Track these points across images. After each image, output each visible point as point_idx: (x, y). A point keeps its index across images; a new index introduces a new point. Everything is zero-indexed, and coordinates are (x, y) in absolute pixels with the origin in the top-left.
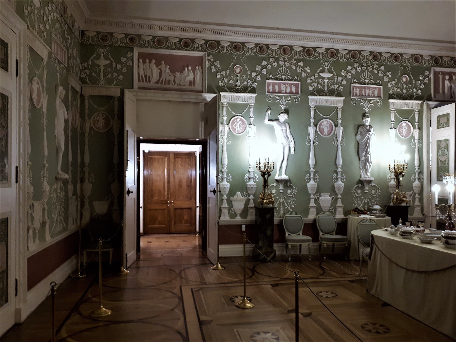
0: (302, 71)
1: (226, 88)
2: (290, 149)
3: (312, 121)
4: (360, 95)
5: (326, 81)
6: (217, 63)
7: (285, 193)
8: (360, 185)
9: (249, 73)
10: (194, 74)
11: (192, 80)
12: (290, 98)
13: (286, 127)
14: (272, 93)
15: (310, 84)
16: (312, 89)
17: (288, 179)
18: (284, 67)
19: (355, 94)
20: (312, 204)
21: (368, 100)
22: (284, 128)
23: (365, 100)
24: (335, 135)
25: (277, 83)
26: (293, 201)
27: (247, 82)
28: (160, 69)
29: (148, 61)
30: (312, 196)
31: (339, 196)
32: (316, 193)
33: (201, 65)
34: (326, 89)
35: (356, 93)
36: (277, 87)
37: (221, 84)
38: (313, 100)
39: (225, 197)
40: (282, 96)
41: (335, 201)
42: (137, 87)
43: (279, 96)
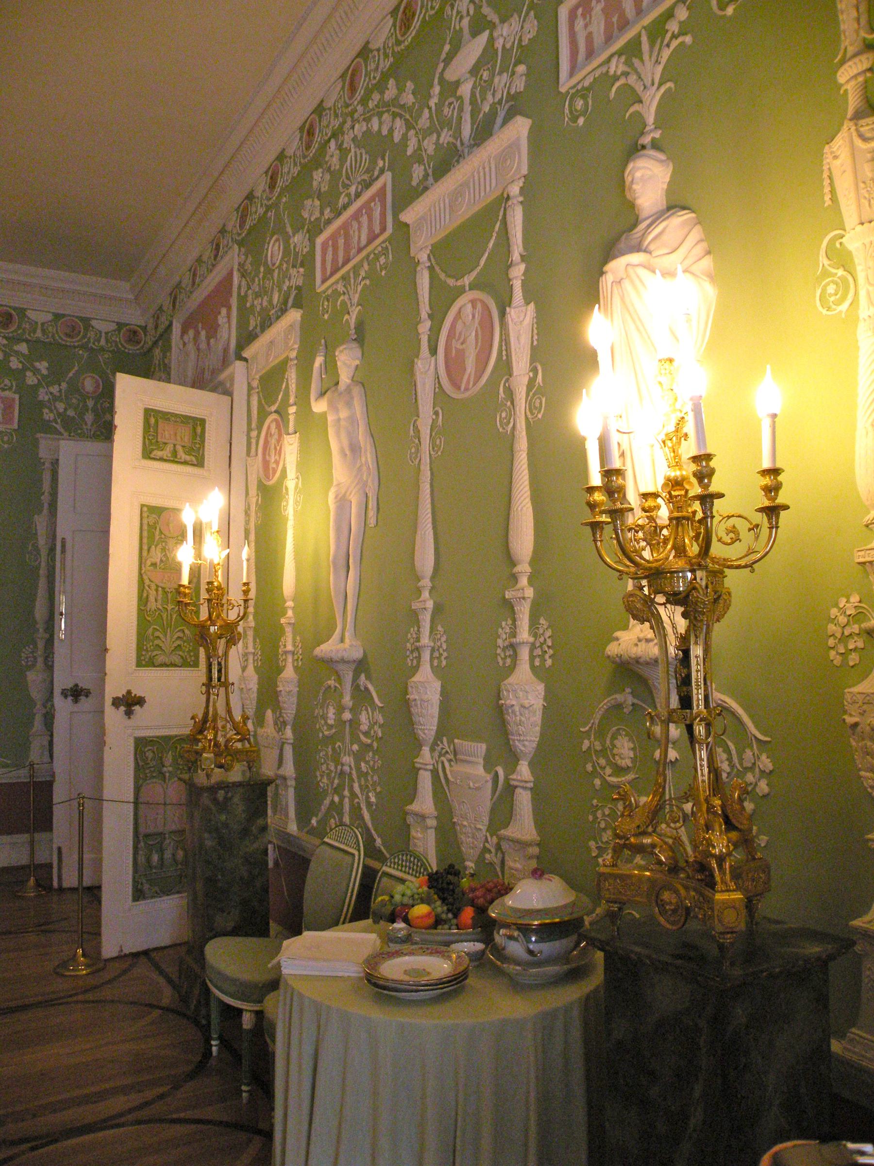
0: (395, 115)
3: (425, 327)
5: (465, 90)
7: (354, 723)
8: (626, 698)
13: (349, 404)
17: (358, 654)
18: (353, 150)
20: (424, 803)
22: (344, 414)
23: (632, 50)
24: (505, 366)
28: (198, 349)
30: (426, 756)
31: (524, 771)
32: (438, 737)
35: (589, 38)
40: (348, 272)
41: (504, 799)
43: (343, 278)
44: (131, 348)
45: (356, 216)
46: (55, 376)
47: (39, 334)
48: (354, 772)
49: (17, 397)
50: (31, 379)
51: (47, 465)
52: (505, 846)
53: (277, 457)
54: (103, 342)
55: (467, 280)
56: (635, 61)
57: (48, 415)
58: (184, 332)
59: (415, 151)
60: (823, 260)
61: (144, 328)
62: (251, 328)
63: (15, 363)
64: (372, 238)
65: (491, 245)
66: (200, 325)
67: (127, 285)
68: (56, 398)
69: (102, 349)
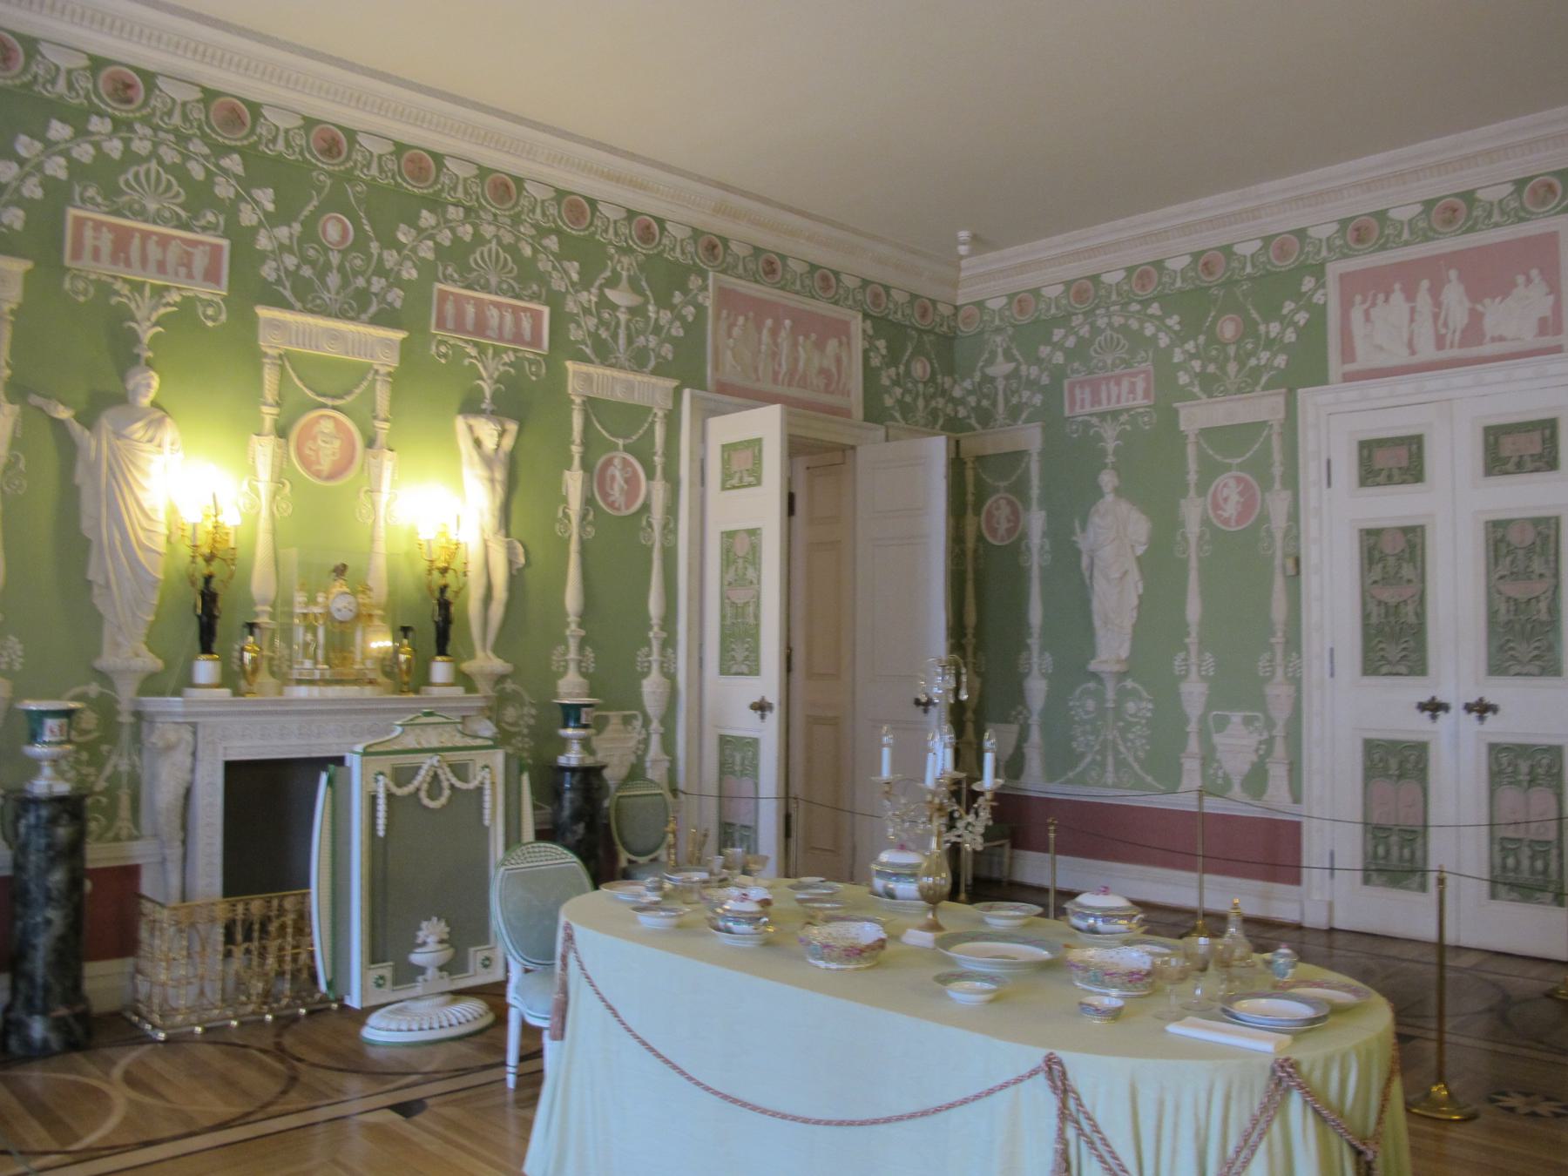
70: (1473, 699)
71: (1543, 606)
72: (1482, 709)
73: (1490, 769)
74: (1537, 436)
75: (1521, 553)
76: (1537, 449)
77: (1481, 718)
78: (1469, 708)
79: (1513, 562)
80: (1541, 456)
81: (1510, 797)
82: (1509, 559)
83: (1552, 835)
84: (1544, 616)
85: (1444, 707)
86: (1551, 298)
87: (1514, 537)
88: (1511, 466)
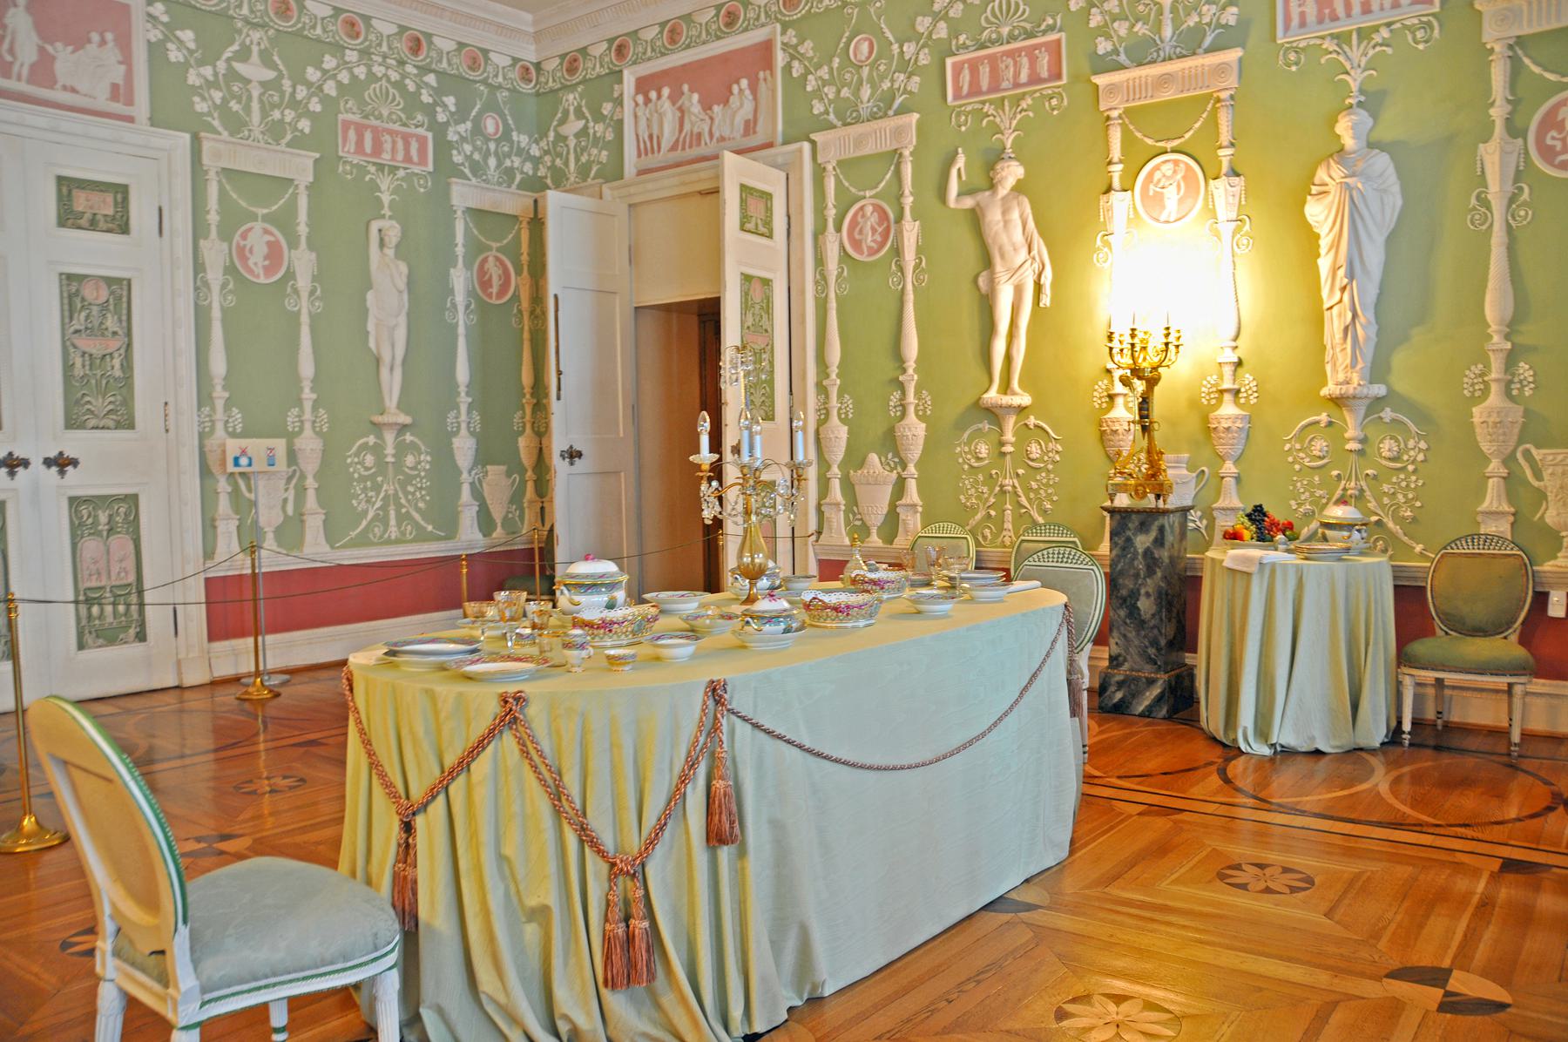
1: (832, 117)
2: (1038, 287)
4: (1320, 21)
6: (807, 48)
9: (896, 47)
10: (755, 98)
11: (751, 117)
12: (1029, 101)
14: (970, 95)
15: (1104, 31)
16: (1109, 47)
19: (1295, 22)
21: (1359, 30)
25: (988, 57)
26: (1048, 485)
27: (892, 81)
28: (681, 109)
29: (653, 95)
33: (769, 64)
34: (1168, 32)
35: (1302, 15)
36: (985, 71)
37: (818, 108)
38: (1112, 89)
39: (835, 470)
40: (1003, 99)
42: (634, 171)
43: (991, 102)
44: (528, 88)
45: (1009, 54)
46: (460, 116)
47: (444, 65)
48: (1020, 492)
49: (430, 135)
50: (442, 117)
51: (459, 213)
52: (1215, 513)
53: (878, 238)
54: (500, 79)
55: (1170, 145)
56: (1346, 48)
57: (457, 159)
58: (643, 85)
59: (1098, 27)
60: (1473, 201)
61: (538, 66)
62: (816, 112)
63: (426, 98)
64: (1035, 79)
65: (1197, 125)
66: (686, 87)
67: (529, 17)
68: (463, 139)
69: (500, 87)
70: (52, 454)
71: (117, 362)
72: (61, 463)
73: (72, 522)
74: (109, 198)
75: (95, 310)
76: (110, 211)
77: (62, 473)
78: (48, 462)
79: (87, 317)
80: (114, 218)
81: (91, 547)
82: (83, 314)
83: (132, 578)
84: (118, 373)
85: (25, 463)
86: (123, 68)
87: (88, 292)
88: (84, 222)
